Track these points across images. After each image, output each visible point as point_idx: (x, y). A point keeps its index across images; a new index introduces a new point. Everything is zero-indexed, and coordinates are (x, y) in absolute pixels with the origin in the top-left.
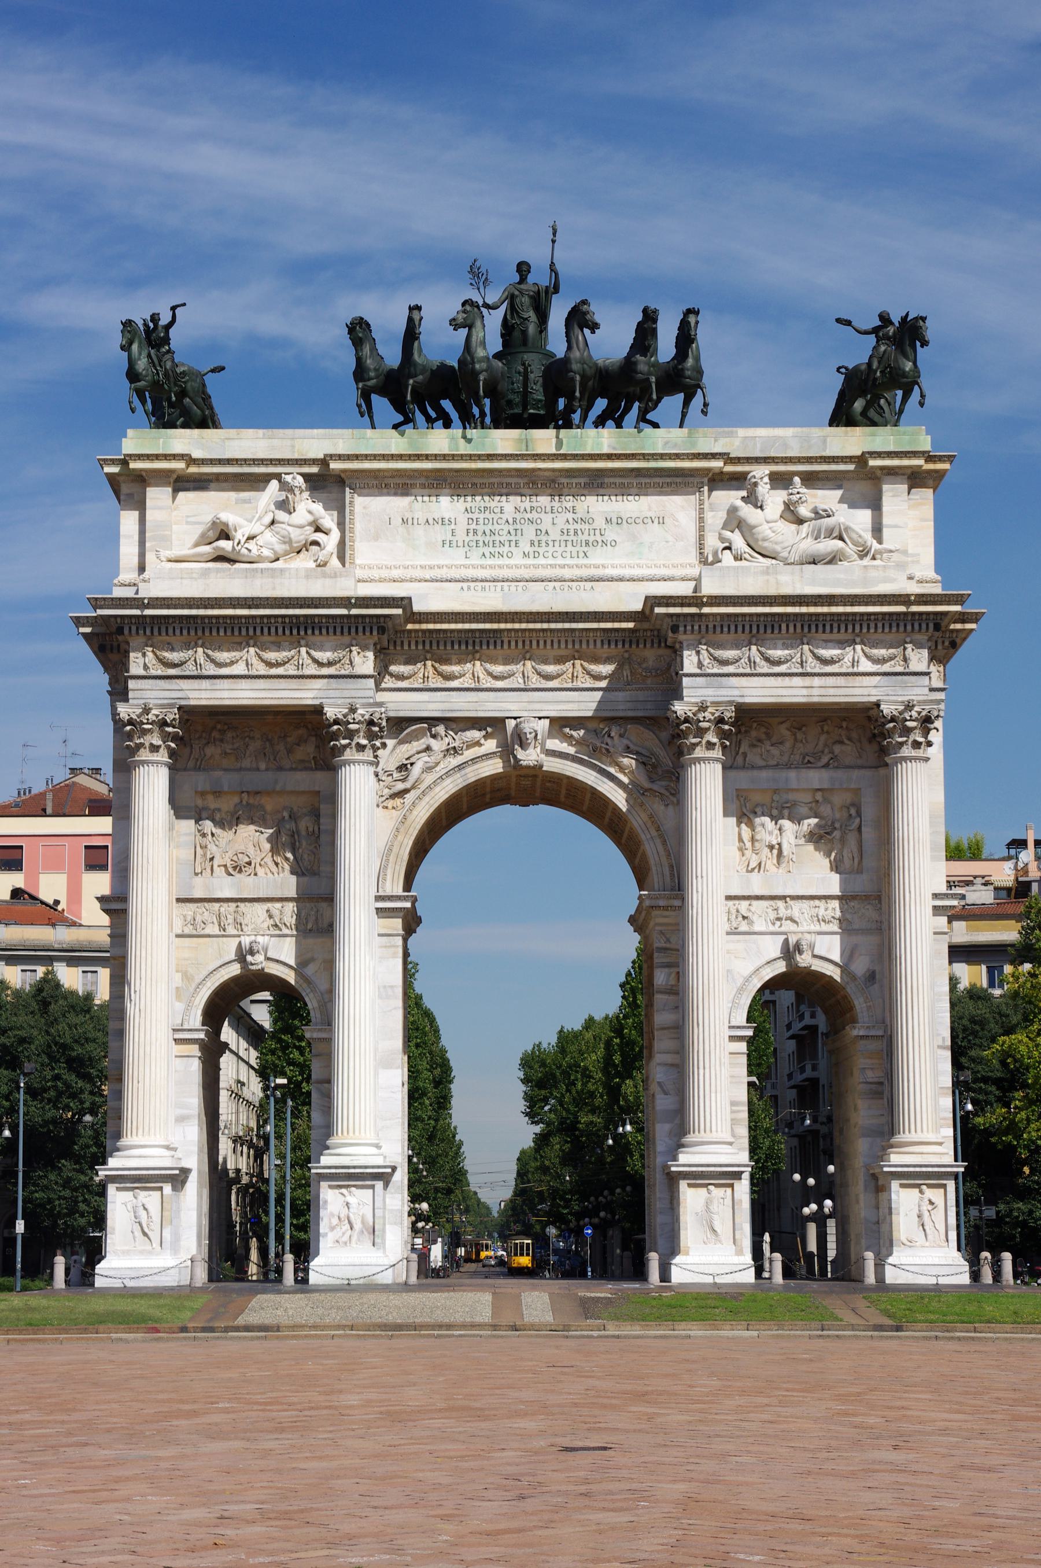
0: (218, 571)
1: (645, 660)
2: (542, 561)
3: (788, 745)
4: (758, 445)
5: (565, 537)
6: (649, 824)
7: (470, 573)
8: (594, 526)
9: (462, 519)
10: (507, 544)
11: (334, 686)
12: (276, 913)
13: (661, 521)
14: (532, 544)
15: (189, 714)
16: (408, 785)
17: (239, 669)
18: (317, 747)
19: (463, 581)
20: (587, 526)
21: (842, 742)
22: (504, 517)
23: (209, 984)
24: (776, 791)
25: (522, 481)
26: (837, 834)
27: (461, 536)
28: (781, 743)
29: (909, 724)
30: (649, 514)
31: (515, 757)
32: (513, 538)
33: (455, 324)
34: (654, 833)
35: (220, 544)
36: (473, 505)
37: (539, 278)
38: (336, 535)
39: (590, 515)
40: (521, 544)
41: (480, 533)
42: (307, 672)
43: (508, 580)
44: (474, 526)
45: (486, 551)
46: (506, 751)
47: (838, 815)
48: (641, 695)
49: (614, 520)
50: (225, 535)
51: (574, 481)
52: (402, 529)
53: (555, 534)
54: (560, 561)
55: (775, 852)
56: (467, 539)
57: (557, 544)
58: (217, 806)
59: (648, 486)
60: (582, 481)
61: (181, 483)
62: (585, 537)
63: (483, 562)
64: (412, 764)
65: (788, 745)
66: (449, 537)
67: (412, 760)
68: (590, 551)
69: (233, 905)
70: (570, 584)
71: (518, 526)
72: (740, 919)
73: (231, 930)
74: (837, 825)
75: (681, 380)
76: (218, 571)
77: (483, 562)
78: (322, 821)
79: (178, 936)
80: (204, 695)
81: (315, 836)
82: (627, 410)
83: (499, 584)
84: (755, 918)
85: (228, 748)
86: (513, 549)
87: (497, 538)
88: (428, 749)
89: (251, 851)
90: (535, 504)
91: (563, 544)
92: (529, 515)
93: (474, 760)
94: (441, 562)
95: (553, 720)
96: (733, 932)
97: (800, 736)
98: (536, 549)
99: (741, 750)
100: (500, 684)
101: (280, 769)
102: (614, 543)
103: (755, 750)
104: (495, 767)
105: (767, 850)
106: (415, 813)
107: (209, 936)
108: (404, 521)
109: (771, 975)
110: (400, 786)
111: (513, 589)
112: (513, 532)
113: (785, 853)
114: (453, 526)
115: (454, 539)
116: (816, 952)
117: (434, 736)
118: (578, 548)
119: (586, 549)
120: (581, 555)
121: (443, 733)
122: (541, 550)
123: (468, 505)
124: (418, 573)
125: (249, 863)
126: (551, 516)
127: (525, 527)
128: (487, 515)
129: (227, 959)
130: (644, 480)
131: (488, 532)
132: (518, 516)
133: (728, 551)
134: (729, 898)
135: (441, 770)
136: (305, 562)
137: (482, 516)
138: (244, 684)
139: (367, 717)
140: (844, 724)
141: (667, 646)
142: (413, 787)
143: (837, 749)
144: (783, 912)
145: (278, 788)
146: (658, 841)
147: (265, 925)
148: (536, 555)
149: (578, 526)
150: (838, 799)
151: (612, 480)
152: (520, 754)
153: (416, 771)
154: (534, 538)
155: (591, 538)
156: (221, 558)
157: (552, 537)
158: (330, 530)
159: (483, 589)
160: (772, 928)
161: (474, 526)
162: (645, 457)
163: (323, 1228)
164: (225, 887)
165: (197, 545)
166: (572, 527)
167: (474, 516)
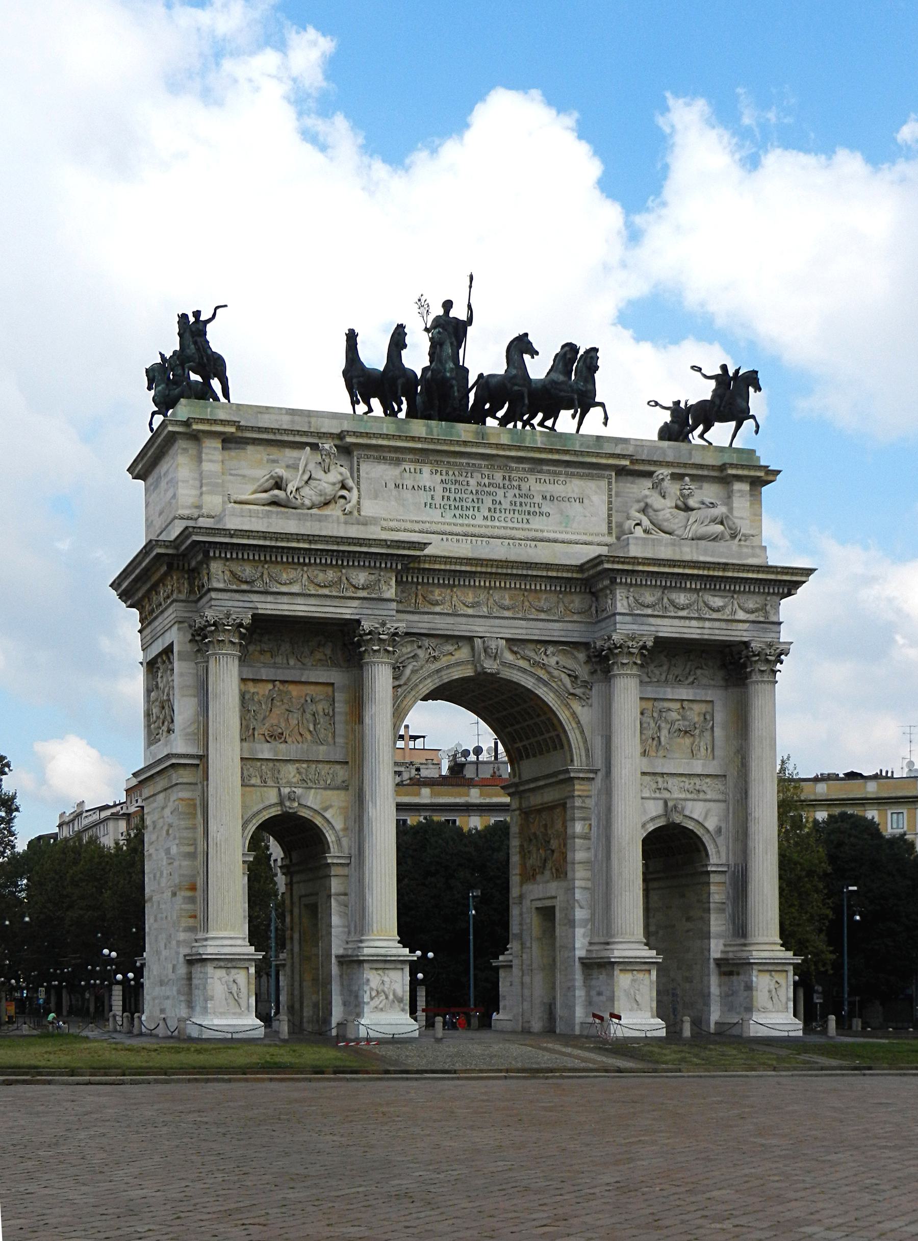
0: (277, 513)
1: (572, 602)
2: (497, 523)
3: (665, 668)
4: (645, 451)
5: (513, 507)
6: (571, 719)
7: (448, 528)
8: (532, 501)
9: (439, 489)
10: (472, 509)
11: (367, 606)
13: (581, 501)
14: (490, 510)
15: (258, 619)
16: (402, 682)
17: (295, 589)
18: (332, 650)
19: (443, 534)
20: (529, 500)
21: (702, 668)
22: (470, 488)
23: (254, 821)
24: (655, 699)
25: (483, 463)
26: (697, 732)
27: (438, 500)
28: (661, 666)
31: (482, 666)
32: (476, 505)
34: (574, 725)
36: (447, 478)
39: (532, 493)
40: (482, 510)
41: (452, 499)
42: (348, 594)
43: (475, 536)
44: (447, 494)
45: (457, 513)
46: (474, 661)
48: (570, 626)
49: (548, 497)
51: (522, 466)
52: (395, 492)
53: (506, 505)
54: (510, 525)
56: (442, 504)
57: (507, 512)
58: (255, 690)
59: (573, 475)
60: (526, 466)
62: (528, 508)
63: (454, 521)
65: (665, 668)
66: (430, 501)
68: (531, 518)
69: (271, 764)
71: (480, 497)
74: (697, 726)
75: (584, 400)
76: (277, 513)
77: (454, 521)
78: (336, 705)
80: (269, 606)
85: (265, 647)
87: (464, 504)
89: (283, 725)
90: (491, 481)
91: (512, 512)
92: (487, 489)
93: (448, 667)
94: (424, 519)
95: (507, 640)
100: (470, 611)
106: (405, 703)
107: (253, 786)
108: (397, 486)
111: (479, 543)
114: (432, 493)
115: (433, 502)
117: (420, 647)
118: (523, 516)
119: (528, 517)
120: (525, 521)
121: (427, 645)
122: (496, 515)
123: (444, 478)
124: (409, 526)
126: (503, 491)
127: (484, 498)
128: (457, 486)
129: (267, 803)
130: (570, 470)
131: (458, 499)
132: (479, 488)
133: (639, 527)
135: (424, 673)
137: (453, 487)
138: (300, 600)
139: (392, 630)
140: (704, 655)
141: (590, 592)
142: (405, 684)
143: (699, 672)
145: (303, 680)
146: (577, 732)
148: (493, 519)
149: (523, 500)
151: (548, 468)
154: (490, 505)
155: (532, 510)
157: (504, 507)
158: (352, 488)
159: (458, 541)
161: (447, 494)
162: (566, 452)
163: (366, 999)
164: (265, 751)
167: (448, 486)
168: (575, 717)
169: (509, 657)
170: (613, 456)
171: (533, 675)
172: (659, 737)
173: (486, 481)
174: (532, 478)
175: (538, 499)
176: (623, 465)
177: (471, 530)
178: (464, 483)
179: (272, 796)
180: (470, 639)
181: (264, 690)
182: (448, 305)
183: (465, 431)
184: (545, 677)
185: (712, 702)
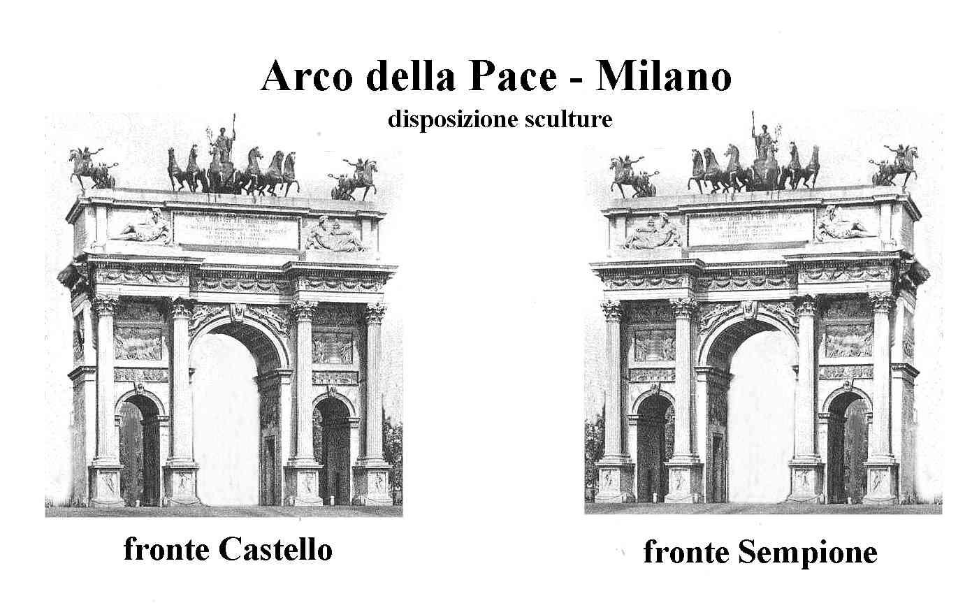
29: (378, 312)
35: (131, 234)
37: (228, 134)
38: (171, 231)
46: (231, 315)
50: (132, 230)
61: (109, 207)
67: (196, 318)
75: (288, 180)
82: (263, 188)
95: (248, 305)
100: (228, 291)
136: (161, 241)
152: (236, 317)
156: (131, 239)
165: (122, 234)
168: (280, 344)
169: (247, 313)
170: (300, 208)
179: (130, 387)
180: (229, 304)
182: (223, 130)
183: (226, 198)
184: (267, 323)
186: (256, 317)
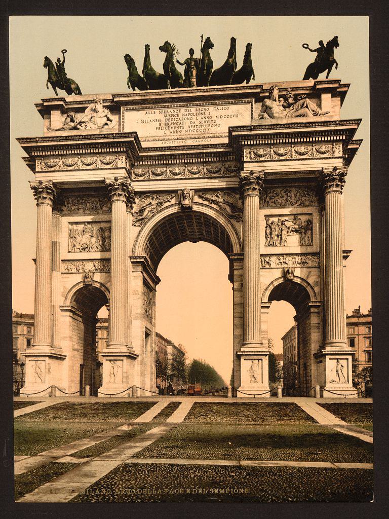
3: (284, 199)
12: (96, 265)
13: (237, 116)
16: (143, 217)
27: (163, 125)
30: (232, 114)
33: (162, 49)
45: (172, 130)
46: (180, 203)
47: (303, 224)
55: (279, 238)
62: (209, 123)
64: (145, 209)
66: (158, 126)
70: (202, 139)
72: (266, 263)
73: (81, 271)
79: (62, 273)
81: (110, 237)
83: (176, 141)
84: (271, 263)
86: (182, 129)
87: (176, 125)
88: (150, 203)
90: (190, 113)
91: (200, 127)
92: (188, 117)
93: (167, 207)
96: (263, 268)
97: (289, 194)
98: (190, 129)
99: (267, 200)
101: (98, 213)
102: (219, 125)
103: (272, 200)
104: (175, 209)
105: (276, 238)
108: (142, 122)
109: (277, 284)
110: (141, 218)
112: (182, 123)
113: (283, 238)
116: (295, 275)
117: (153, 199)
119: (208, 128)
125: (87, 248)
127: (186, 121)
132: (184, 117)
134: (261, 255)
143: (303, 199)
144: (282, 261)
147: (93, 269)
149: (205, 120)
150: (304, 218)
152: (184, 203)
153: (146, 212)
160: (278, 266)
161: (168, 122)
166: (204, 120)
171: (211, 208)
172: (281, 235)
173: (187, 113)
174: (211, 108)
175: (214, 118)
176: (259, 96)
177: (179, 137)
178: (176, 115)
181: (81, 227)
185: (311, 214)
186: (207, 203)
